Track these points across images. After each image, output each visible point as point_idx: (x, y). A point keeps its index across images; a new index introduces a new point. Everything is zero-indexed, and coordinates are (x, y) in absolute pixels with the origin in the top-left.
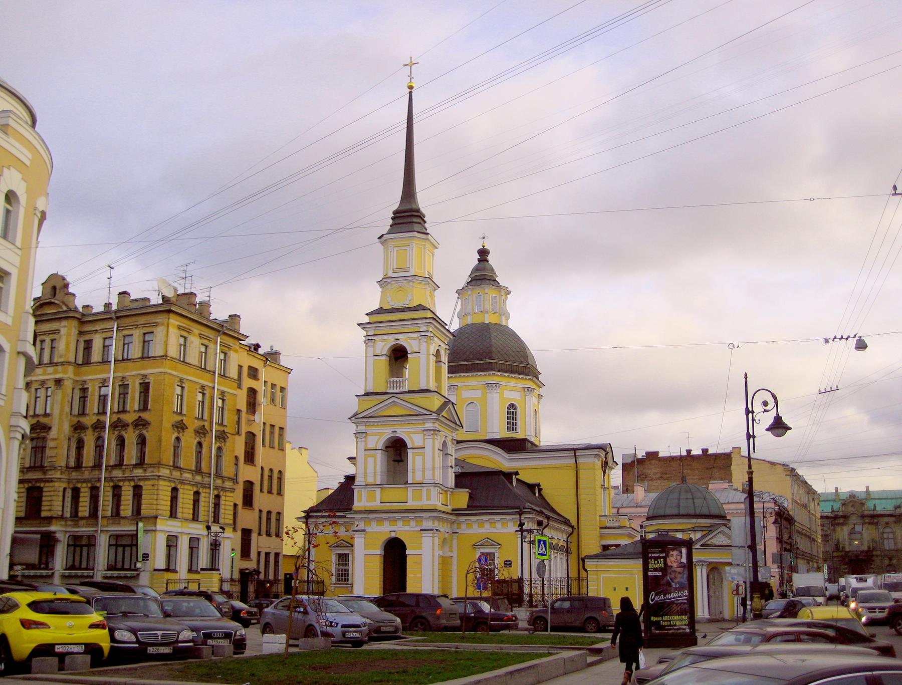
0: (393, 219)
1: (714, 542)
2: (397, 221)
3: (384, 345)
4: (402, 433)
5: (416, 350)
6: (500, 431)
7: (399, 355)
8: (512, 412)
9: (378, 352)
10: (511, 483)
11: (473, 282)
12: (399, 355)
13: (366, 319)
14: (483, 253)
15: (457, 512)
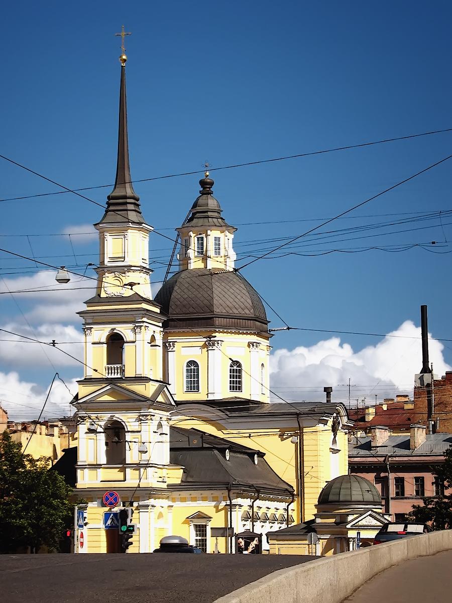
0: (109, 204)
1: (363, 523)
2: (111, 208)
3: (101, 333)
4: (120, 416)
5: (132, 339)
6: (221, 391)
7: (115, 344)
8: (236, 371)
9: (97, 340)
10: (225, 457)
11: (195, 221)
12: (115, 344)
13: (85, 308)
14: (206, 187)
15: (172, 488)
